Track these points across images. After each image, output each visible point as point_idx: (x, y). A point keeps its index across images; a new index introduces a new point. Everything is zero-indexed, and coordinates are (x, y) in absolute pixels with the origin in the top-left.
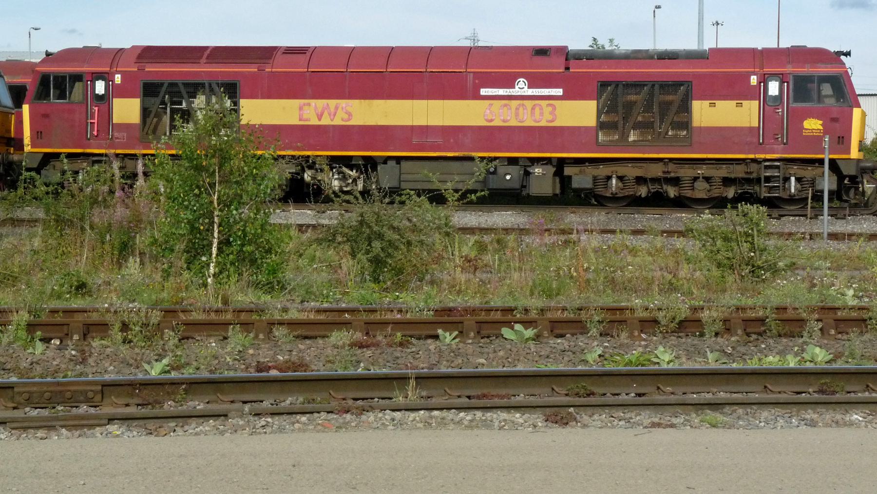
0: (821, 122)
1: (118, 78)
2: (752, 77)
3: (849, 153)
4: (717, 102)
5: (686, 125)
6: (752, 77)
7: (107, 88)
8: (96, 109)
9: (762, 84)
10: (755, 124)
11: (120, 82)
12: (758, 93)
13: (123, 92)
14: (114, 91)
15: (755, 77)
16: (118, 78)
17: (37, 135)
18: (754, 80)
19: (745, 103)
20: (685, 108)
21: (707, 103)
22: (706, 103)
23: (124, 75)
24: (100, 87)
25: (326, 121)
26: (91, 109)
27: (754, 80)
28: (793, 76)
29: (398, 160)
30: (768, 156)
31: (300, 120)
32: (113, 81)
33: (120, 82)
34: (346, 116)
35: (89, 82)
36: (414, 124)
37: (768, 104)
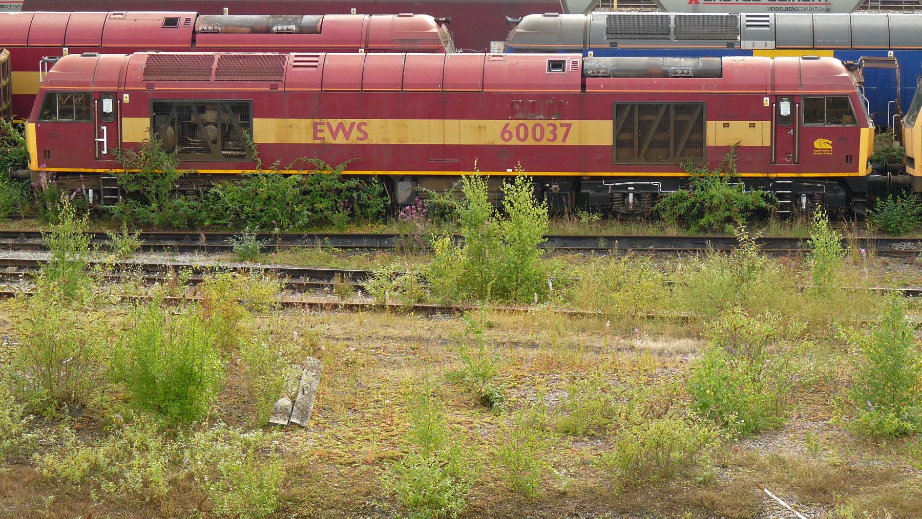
0: (830, 142)
1: (126, 98)
2: (765, 99)
3: (858, 172)
4: (730, 122)
5: (701, 142)
6: (765, 99)
7: (115, 104)
8: (105, 128)
9: (774, 105)
10: (767, 143)
11: (128, 102)
12: (772, 114)
13: (134, 111)
14: (121, 111)
15: (768, 99)
16: (126, 98)
17: (44, 154)
18: (766, 101)
19: (758, 123)
20: (700, 129)
21: (721, 123)
22: (720, 123)
23: (132, 94)
24: (108, 106)
25: (341, 140)
26: (99, 128)
27: (766, 101)
28: (806, 100)
29: (415, 179)
30: (780, 175)
31: (315, 138)
32: (121, 101)
33: (128, 102)
34: (361, 135)
35: (96, 101)
36: (431, 143)
37: (780, 124)
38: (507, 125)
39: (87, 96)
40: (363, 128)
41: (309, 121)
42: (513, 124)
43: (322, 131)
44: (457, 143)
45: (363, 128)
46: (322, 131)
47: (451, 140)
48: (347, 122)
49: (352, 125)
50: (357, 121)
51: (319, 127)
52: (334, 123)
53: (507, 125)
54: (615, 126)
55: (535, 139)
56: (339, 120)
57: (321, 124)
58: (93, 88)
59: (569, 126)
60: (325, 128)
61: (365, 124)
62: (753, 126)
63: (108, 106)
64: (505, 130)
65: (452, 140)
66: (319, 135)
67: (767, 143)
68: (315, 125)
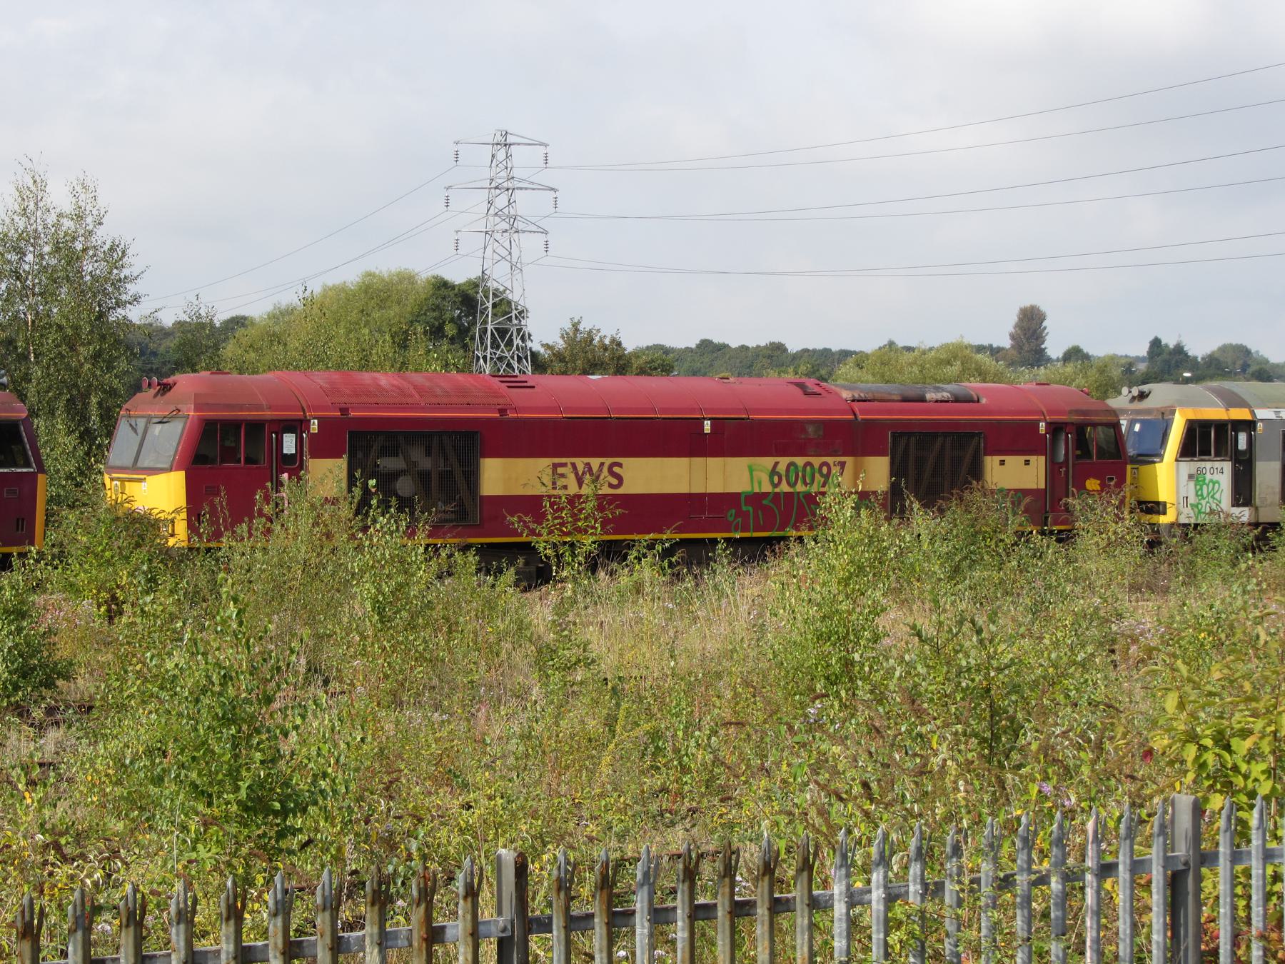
7: (299, 443)
10: (1042, 486)
13: (323, 447)
19: (1033, 459)
22: (997, 459)
38: (776, 464)
39: (256, 427)
40: (616, 469)
41: (545, 462)
42: (784, 462)
43: (562, 476)
44: (683, 488)
45: (616, 469)
46: (562, 476)
47: (715, 487)
48: (595, 462)
49: (602, 464)
50: (608, 461)
51: (560, 470)
52: (580, 462)
53: (776, 464)
54: (892, 463)
55: (788, 483)
56: (586, 460)
57: (564, 465)
58: (268, 414)
59: (843, 465)
60: (566, 470)
61: (620, 465)
62: (1027, 462)
63: (289, 444)
64: (774, 471)
65: (715, 486)
66: (561, 482)
67: (1042, 486)
68: (555, 466)
